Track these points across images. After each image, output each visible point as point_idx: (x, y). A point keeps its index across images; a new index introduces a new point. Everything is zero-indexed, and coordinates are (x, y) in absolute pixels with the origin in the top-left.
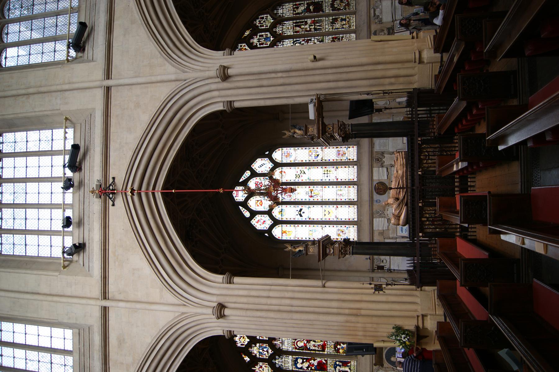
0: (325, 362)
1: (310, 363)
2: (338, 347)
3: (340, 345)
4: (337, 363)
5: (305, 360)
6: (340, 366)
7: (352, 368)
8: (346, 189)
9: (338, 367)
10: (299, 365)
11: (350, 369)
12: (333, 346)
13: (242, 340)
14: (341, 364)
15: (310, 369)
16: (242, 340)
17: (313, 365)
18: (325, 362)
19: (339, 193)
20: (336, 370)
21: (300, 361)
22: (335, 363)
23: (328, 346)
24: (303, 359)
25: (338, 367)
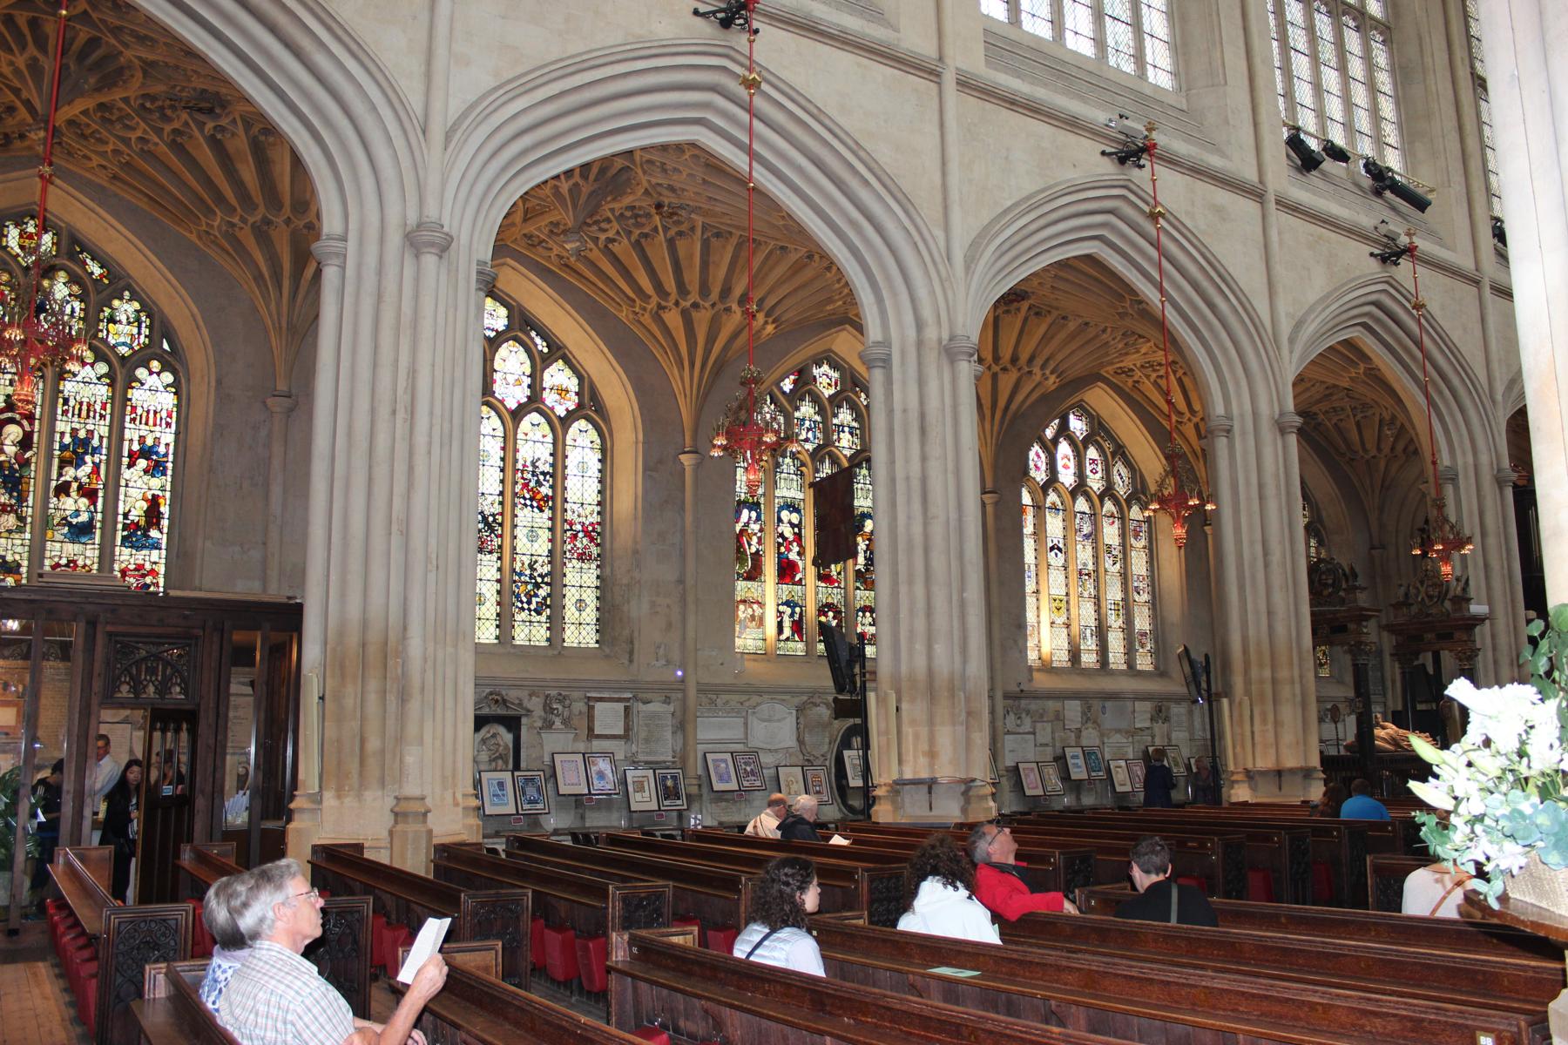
0: (797, 579)
1: (791, 543)
2: (831, 614)
3: (834, 618)
4: (798, 610)
5: (796, 530)
6: (792, 615)
7: (790, 644)
8: (1094, 647)
9: (789, 611)
10: (785, 515)
11: (787, 639)
12: (830, 600)
13: (825, 381)
14: (796, 617)
15: (780, 540)
16: (825, 381)
17: (789, 550)
18: (797, 579)
19: (1088, 632)
20: (783, 604)
21: (795, 518)
22: (796, 605)
23: (830, 590)
24: (799, 526)
25: (789, 611)
